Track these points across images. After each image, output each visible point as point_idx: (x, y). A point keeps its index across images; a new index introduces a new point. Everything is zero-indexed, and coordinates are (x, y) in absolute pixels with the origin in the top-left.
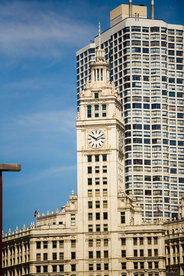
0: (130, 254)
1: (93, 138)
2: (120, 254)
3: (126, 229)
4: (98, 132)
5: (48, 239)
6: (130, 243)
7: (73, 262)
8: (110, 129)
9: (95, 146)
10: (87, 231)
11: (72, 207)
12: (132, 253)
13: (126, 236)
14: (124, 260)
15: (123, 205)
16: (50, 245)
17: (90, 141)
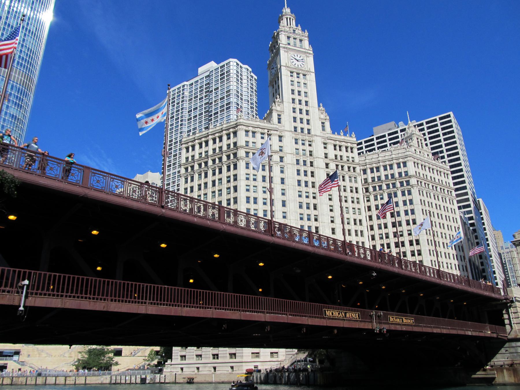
0: (331, 156)
1: (295, 59)
2: (324, 155)
3: (327, 135)
4: (299, 56)
5: (256, 130)
6: (330, 147)
7: (281, 154)
8: (308, 57)
9: (296, 66)
10: (293, 130)
11: (278, 108)
12: (334, 157)
13: (328, 141)
14: (327, 161)
15: (322, 116)
16: (258, 136)
17: (292, 61)
